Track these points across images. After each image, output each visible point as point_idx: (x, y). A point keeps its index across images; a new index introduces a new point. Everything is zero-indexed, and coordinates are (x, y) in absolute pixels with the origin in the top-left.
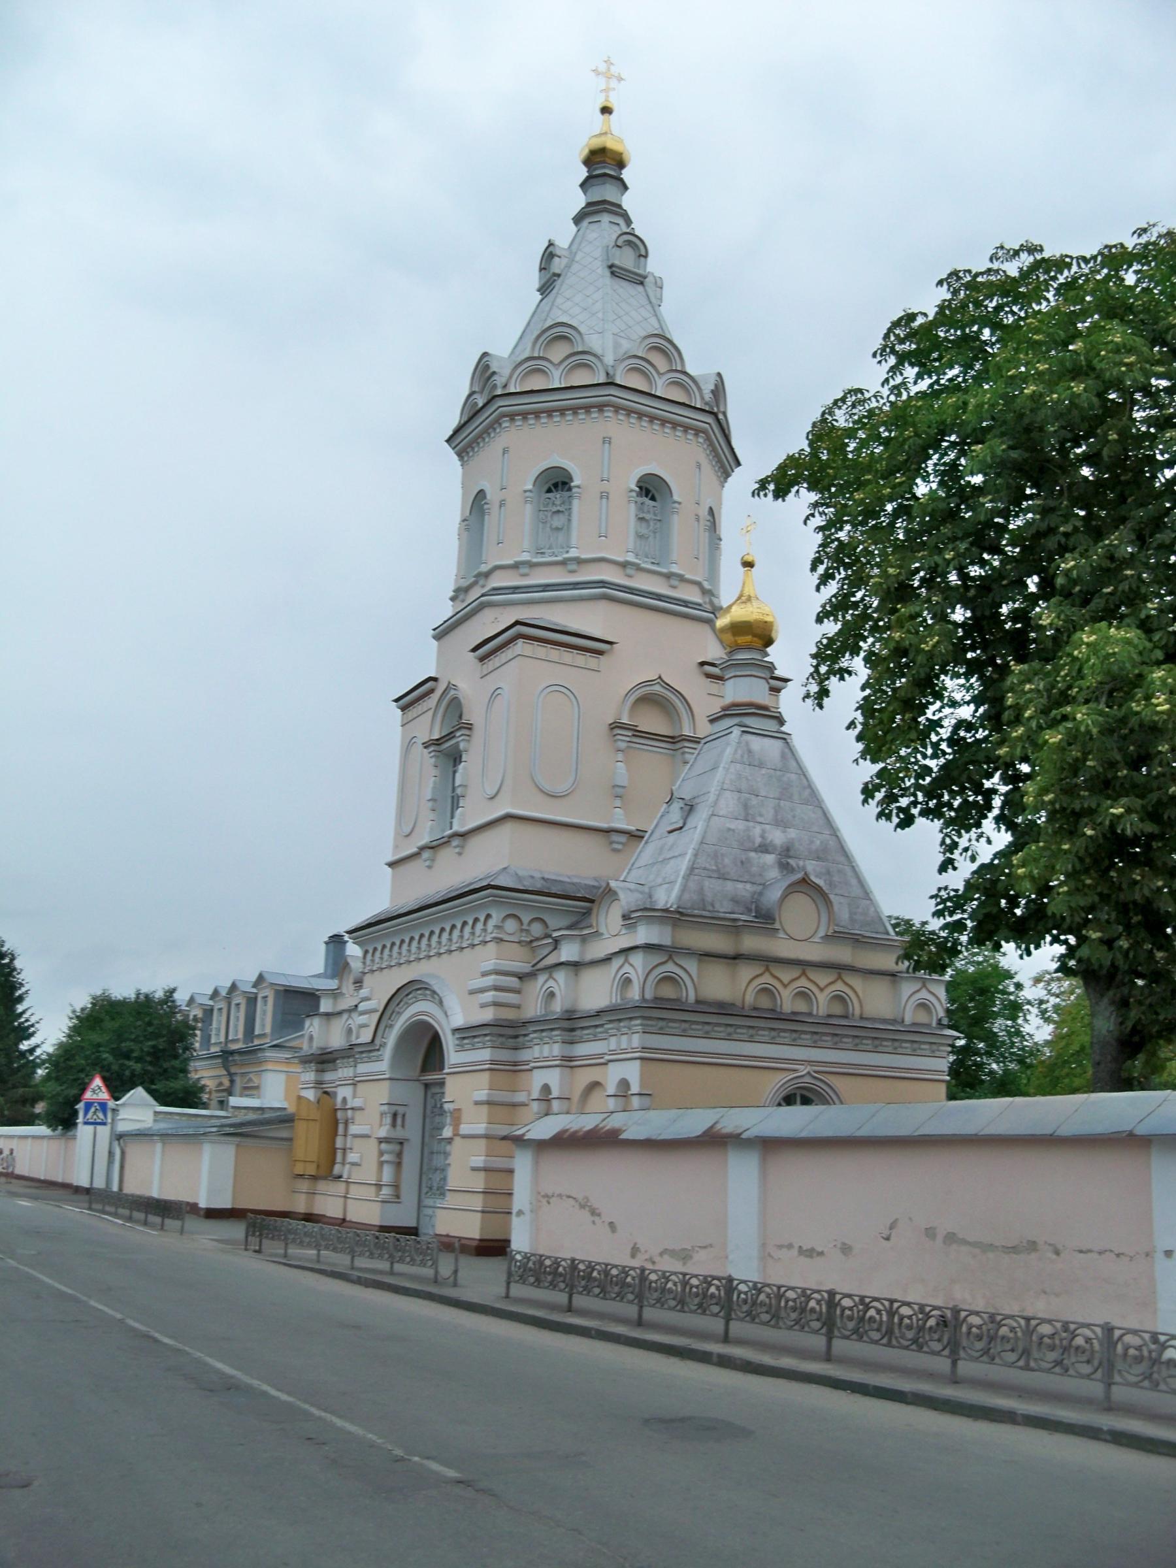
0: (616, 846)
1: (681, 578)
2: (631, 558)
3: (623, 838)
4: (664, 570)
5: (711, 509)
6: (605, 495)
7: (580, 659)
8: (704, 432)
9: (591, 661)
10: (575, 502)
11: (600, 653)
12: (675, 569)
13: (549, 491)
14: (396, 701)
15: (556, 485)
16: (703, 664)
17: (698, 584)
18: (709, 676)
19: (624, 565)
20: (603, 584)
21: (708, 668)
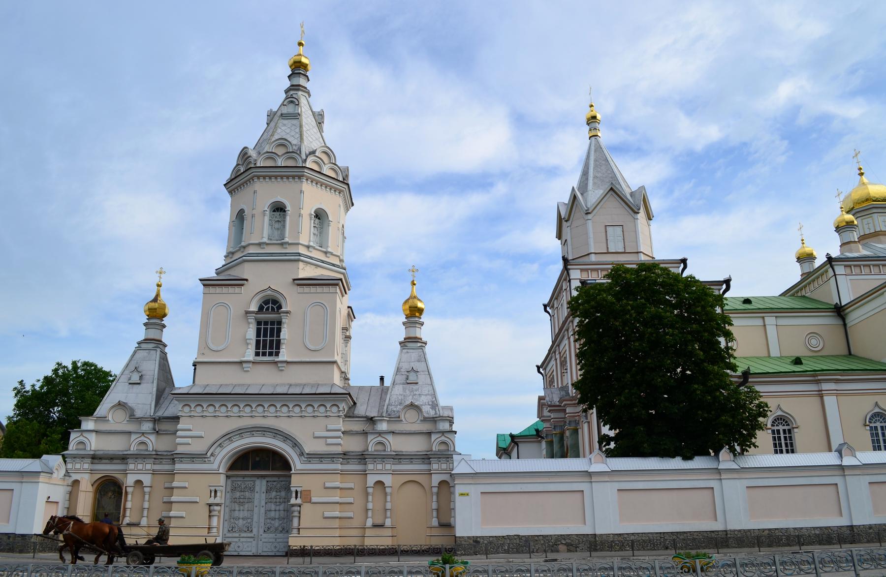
3: (251, 365)
11: (242, 285)
12: (287, 240)
16: (294, 280)
18: (298, 285)
19: (259, 244)
21: (295, 281)
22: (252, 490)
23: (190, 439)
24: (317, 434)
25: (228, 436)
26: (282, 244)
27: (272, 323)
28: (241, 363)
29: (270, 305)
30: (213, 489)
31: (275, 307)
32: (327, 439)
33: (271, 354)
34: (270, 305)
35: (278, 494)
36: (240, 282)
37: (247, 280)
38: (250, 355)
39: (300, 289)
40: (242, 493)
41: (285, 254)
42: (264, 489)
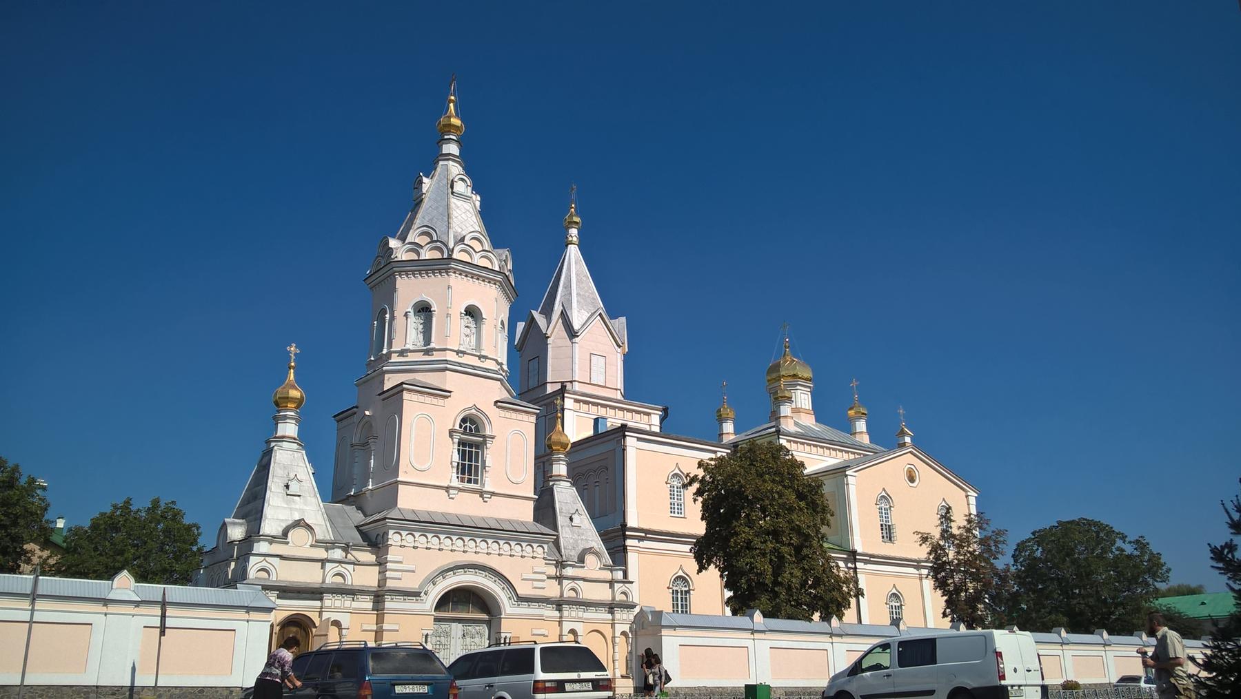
0: (451, 496)
1: (486, 357)
2: (461, 349)
3: (456, 492)
4: (479, 354)
5: (502, 321)
6: (448, 315)
7: (435, 400)
8: (500, 282)
9: (441, 402)
10: (434, 319)
12: (483, 353)
13: (419, 311)
14: (334, 417)
15: (423, 309)
17: (496, 361)
18: (498, 407)
19: (458, 352)
20: (446, 362)
21: (499, 404)
22: (447, 635)
23: (400, 573)
24: (525, 576)
25: (444, 572)
26: (480, 357)
27: (471, 446)
28: (447, 489)
29: (468, 424)
30: (425, 632)
31: (473, 427)
32: (535, 582)
33: (469, 481)
34: (468, 424)
35: (472, 640)
36: (443, 393)
37: (450, 392)
38: (456, 483)
39: (503, 413)
40: (438, 638)
41: (460, 364)
42: (460, 634)
